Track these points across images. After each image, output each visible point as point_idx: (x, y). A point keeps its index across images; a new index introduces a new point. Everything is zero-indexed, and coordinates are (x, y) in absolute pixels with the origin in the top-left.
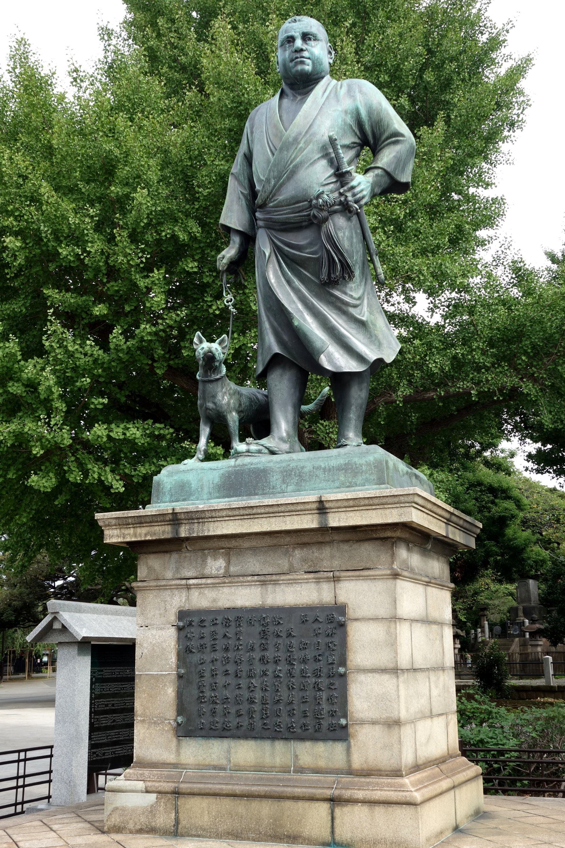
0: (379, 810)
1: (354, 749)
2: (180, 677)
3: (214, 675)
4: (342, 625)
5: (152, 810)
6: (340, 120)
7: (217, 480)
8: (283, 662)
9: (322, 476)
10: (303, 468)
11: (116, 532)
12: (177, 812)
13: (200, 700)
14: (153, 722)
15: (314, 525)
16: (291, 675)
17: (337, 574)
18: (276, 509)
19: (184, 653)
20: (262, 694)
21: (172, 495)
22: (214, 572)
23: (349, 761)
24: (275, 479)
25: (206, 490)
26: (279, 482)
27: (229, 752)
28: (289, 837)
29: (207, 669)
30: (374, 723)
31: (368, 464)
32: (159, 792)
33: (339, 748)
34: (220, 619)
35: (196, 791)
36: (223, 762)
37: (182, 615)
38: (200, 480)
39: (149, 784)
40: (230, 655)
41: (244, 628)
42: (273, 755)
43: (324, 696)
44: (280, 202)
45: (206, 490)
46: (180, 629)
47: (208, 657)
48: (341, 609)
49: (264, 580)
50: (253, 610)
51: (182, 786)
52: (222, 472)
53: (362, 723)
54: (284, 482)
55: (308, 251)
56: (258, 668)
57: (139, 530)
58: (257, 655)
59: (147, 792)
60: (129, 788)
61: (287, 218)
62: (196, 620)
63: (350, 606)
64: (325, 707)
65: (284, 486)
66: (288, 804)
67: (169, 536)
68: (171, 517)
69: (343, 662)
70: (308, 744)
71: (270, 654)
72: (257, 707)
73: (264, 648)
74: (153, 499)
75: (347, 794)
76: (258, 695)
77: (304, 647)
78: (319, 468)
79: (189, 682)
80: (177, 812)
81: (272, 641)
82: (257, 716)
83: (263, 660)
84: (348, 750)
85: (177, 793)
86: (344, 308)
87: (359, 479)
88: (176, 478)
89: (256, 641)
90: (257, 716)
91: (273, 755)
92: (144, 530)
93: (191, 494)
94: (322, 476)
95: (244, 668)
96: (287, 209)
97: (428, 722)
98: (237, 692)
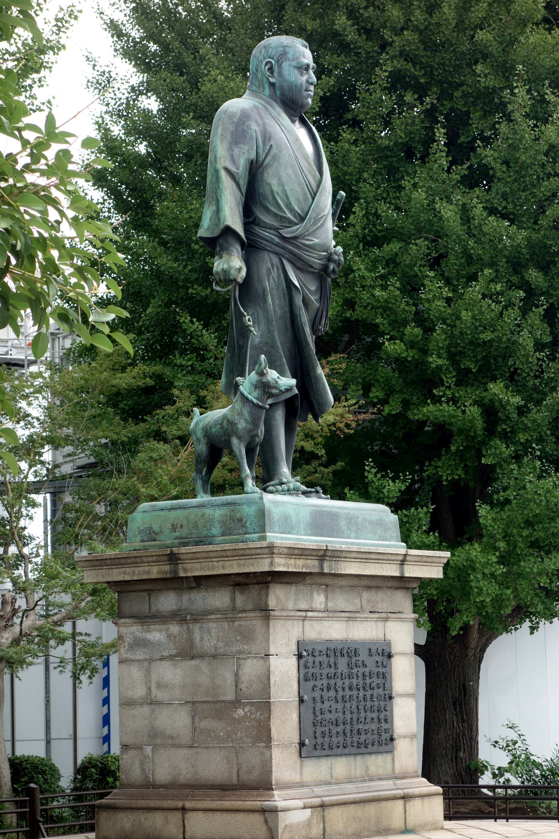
0: (426, 800)
1: (396, 758)
5: (308, 824)
11: (282, 561)
12: (324, 823)
14: (285, 746)
15: (397, 574)
23: (393, 768)
28: (384, 830)
30: (405, 737)
32: (311, 807)
33: (388, 757)
35: (334, 802)
39: (305, 801)
44: (315, 244)
45: (302, 527)
51: (325, 799)
53: (400, 737)
57: (297, 561)
59: (304, 808)
60: (295, 806)
66: (384, 804)
67: (316, 570)
68: (321, 553)
71: (355, 681)
72: (348, 727)
74: (267, 528)
75: (410, 791)
76: (348, 716)
80: (324, 823)
85: (323, 806)
92: (300, 562)
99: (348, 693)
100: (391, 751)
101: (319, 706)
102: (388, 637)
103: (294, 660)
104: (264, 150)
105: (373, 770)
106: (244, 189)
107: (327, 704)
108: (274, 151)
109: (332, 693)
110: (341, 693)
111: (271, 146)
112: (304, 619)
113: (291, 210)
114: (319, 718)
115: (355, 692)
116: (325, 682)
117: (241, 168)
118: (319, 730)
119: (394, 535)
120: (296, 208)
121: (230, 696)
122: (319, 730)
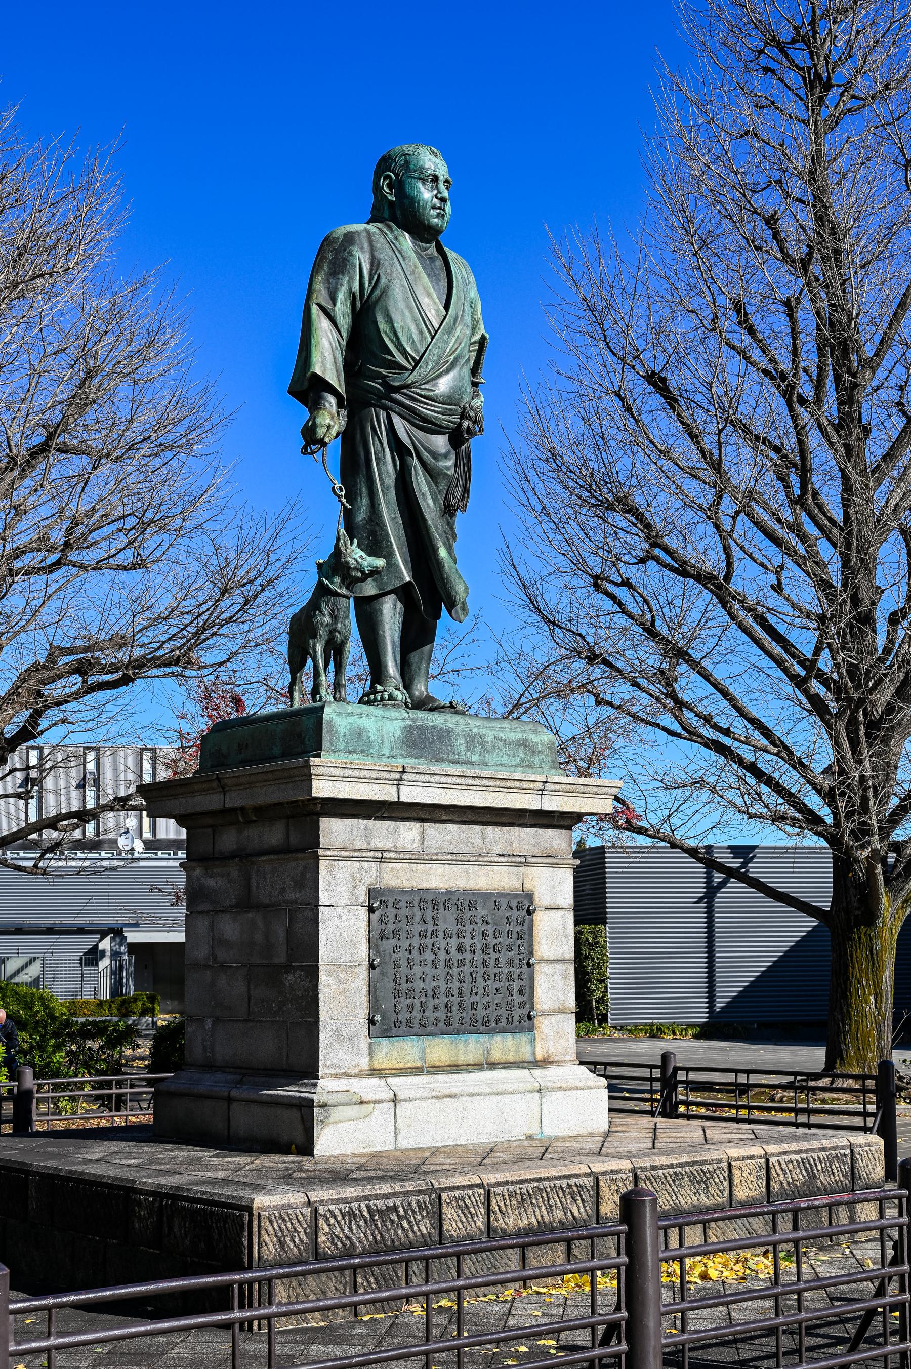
2: (372, 966)
4: (529, 913)
7: (398, 733)
9: (503, 749)
10: (485, 735)
16: (485, 964)
19: (376, 939)
20: (458, 985)
21: (347, 743)
22: (408, 847)
23: (534, 1053)
24: (459, 743)
25: (387, 744)
26: (463, 748)
27: (424, 1052)
29: (402, 956)
31: (543, 744)
33: (524, 1038)
36: (419, 1064)
37: (373, 894)
38: (380, 729)
40: (428, 942)
42: (466, 1053)
43: (516, 988)
45: (387, 744)
46: (371, 910)
47: (405, 944)
48: (530, 897)
49: (456, 858)
50: (449, 893)
52: (403, 724)
56: (455, 956)
58: (454, 942)
61: (436, 418)
62: (391, 900)
63: (536, 895)
64: (517, 999)
65: (468, 754)
69: (531, 953)
70: (498, 1038)
71: (467, 942)
72: (456, 999)
73: (461, 934)
76: (455, 985)
77: (497, 934)
78: (500, 739)
81: (468, 928)
82: (455, 1008)
83: (460, 949)
84: (533, 1042)
87: (536, 759)
88: (351, 720)
89: (454, 928)
90: (455, 1008)
93: (370, 746)
94: (503, 749)
95: (442, 956)
96: (439, 407)
98: (434, 984)
100: (531, 1029)
101: (404, 970)
102: (528, 887)
103: (364, 913)
104: (370, 282)
105: (497, 1055)
106: (344, 330)
107: (417, 970)
108: (383, 281)
109: (429, 956)
110: (442, 956)
111: (379, 276)
112: (382, 860)
113: (404, 353)
114: (405, 986)
115: (468, 956)
116: (416, 942)
117: (338, 304)
119: (548, 759)
120: (409, 350)
121: (280, 958)
122: (404, 1002)
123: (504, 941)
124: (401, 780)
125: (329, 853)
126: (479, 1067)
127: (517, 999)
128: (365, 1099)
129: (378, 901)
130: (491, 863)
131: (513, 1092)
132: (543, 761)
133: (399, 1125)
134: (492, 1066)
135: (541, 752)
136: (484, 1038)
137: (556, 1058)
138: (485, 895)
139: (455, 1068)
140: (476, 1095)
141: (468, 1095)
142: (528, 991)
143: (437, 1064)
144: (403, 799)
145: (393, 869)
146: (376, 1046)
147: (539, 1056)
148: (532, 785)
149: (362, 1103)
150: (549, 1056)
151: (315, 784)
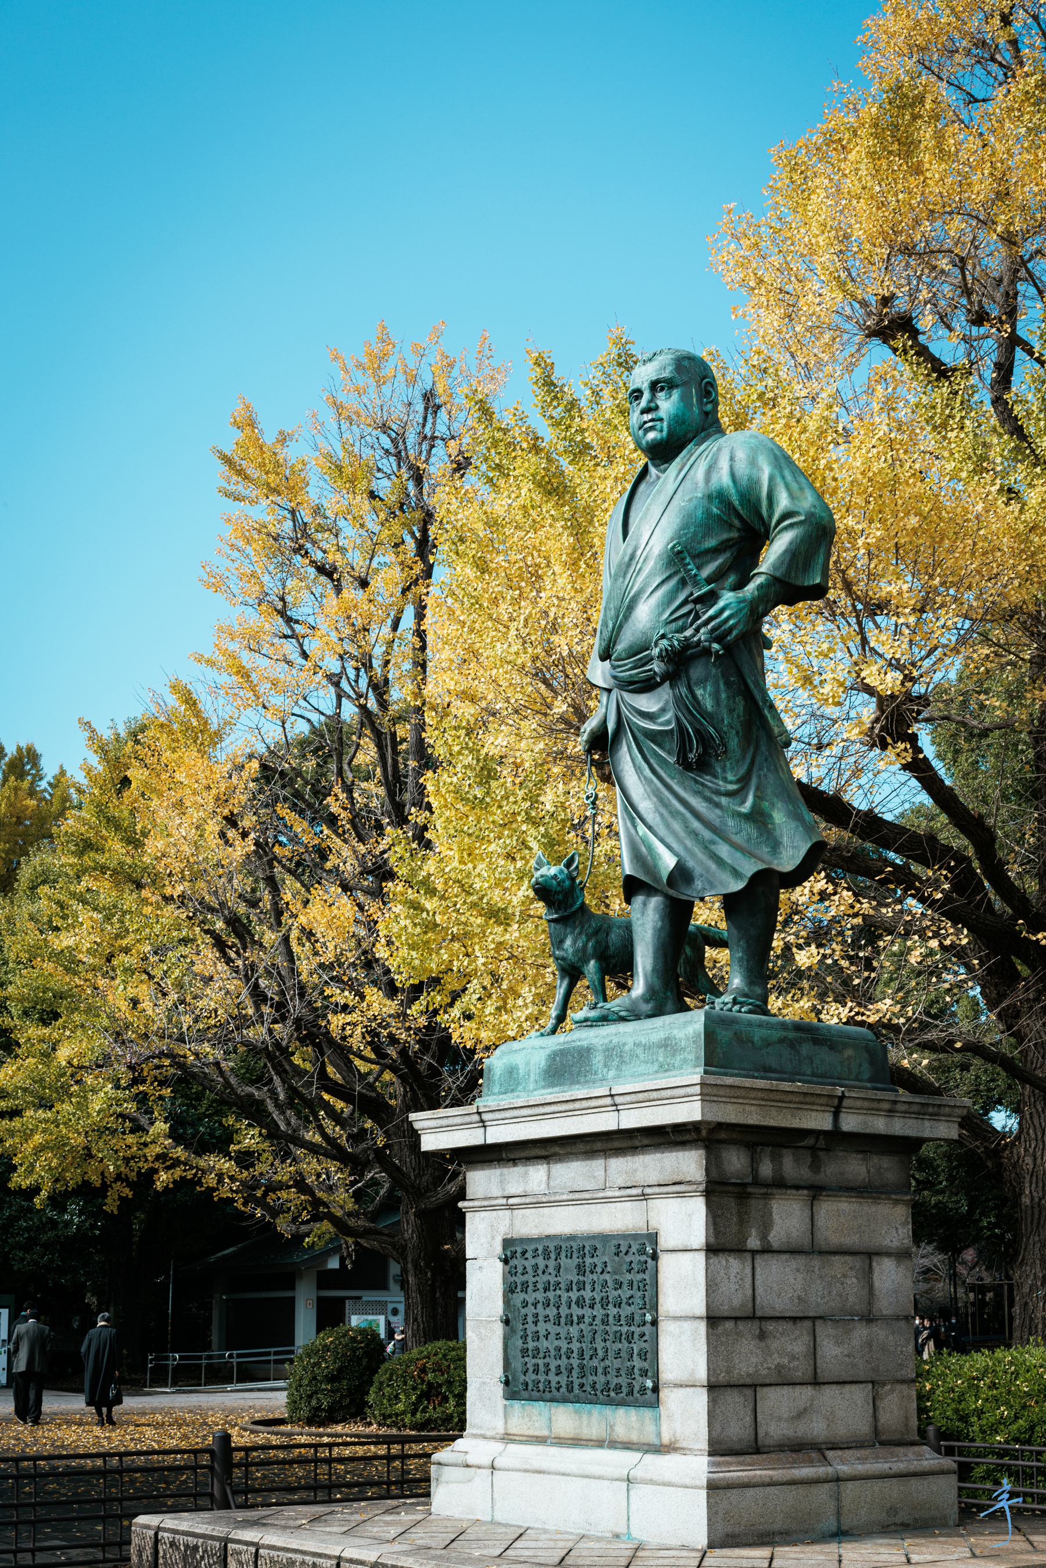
3: (536, 1323)
4: (655, 1257)
6: (699, 513)
7: (543, 1063)
8: (598, 1306)
9: (642, 1056)
10: (624, 1044)
13: (525, 1352)
17: (648, 1191)
18: (570, 1106)
26: (601, 1065)
33: (647, 1413)
34: (530, 1248)
36: (545, 1433)
37: (507, 1243)
40: (551, 1295)
41: (563, 1261)
42: (589, 1425)
46: (506, 1261)
48: (653, 1238)
50: (572, 1238)
54: (606, 1066)
55: (662, 720)
60: (451, 1461)
72: (575, 1362)
73: (581, 1286)
76: (575, 1346)
77: (619, 1285)
79: (513, 1331)
84: (657, 1420)
86: (716, 798)
91: (589, 1425)
97: (808, 1391)
99: (576, 1311)
102: (653, 1224)
105: (621, 1433)
107: (542, 1327)
118: (531, 1362)
119: (691, 1057)
123: (625, 1293)
124: (482, 1121)
125: (476, 1203)
126: (600, 1444)
127: (637, 1363)
128: (470, 1463)
129: (513, 1251)
130: (608, 1200)
131: (600, 1478)
132: (685, 1060)
133: (496, 1496)
134: (614, 1444)
135: (684, 1049)
136: (608, 1411)
137: (684, 1444)
138: (604, 1238)
139: (576, 1442)
140: (564, 1474)
141: (557, 1474)
142: (651, 1355)
143: (562, 1435)
144: (489, 1142)
145: (523, 1215)
146: (509, 1409)
147: (666, 1439)
148: (601, 1102)
149: (468, 1466)
150: (676, 1441)
151: (423, 1138)
